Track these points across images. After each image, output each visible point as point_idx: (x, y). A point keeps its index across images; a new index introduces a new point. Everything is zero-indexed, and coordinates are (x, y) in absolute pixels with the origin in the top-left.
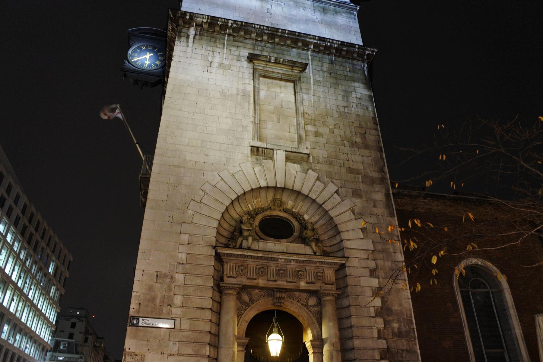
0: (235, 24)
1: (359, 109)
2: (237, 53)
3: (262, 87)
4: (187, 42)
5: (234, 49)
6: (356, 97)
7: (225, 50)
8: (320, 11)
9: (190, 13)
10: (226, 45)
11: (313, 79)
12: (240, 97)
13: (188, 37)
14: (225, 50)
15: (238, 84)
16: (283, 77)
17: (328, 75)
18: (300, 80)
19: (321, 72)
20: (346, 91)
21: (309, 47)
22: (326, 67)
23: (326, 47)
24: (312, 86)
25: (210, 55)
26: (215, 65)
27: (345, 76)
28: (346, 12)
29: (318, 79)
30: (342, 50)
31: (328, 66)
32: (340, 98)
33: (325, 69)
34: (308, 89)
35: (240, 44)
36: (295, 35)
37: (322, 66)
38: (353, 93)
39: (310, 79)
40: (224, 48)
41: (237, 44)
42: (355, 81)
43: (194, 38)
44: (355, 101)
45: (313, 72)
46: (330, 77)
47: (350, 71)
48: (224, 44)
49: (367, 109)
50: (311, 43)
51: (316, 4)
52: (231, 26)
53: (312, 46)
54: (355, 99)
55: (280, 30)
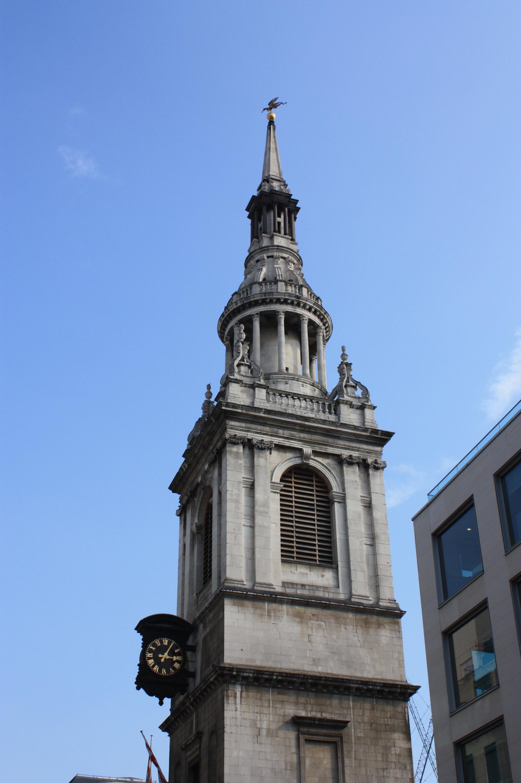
0: (279, 676)
1: (397, 770)
2: (281, 712)
3: (307, 753)
4: (235, 704)
5: (278, 706)
6: (396, 754)
7: (271, 708)
8: (361, 626)
9: (237, 668)
10: (271, 701)
11: (355, 736)
12: (288, 772)
13: (235, 697)
14: (271, 708)
15: (285, 756)
16: (327, 739)
17: (369, 728)
18: (342, 741)
19: (362, 724)
20: (386, 746)
21: (351, 691)
22: (367, 713)
23: (369, 690)
24: (353, 745)
25: (258, 718)
26: (264, 732)
27: (386, 725)
28: (390, 623)
29: (359, 735)
30: (383, 691)
31: (369, 715)
32: (380, 759)
33: (366, 719)
34: (349, 752)
35: (284, 697)
36: (338, 681)
37: (363, 714)
38: (393, 748)
39: (352, 736)
40: (269, 706)
41: (281, 697)
42: (394, 731)
43: (241, 697)
44: (394, 760)
45: (354, 724)
46: (371, 730)
47: (390, 717)
48: (269, 700)
49: (405, 768)
50: (353, 688)
51: (359, 616)
52: (276, 679)
53: (354, 691)
54: (394, 755)
55: (324, 678)
